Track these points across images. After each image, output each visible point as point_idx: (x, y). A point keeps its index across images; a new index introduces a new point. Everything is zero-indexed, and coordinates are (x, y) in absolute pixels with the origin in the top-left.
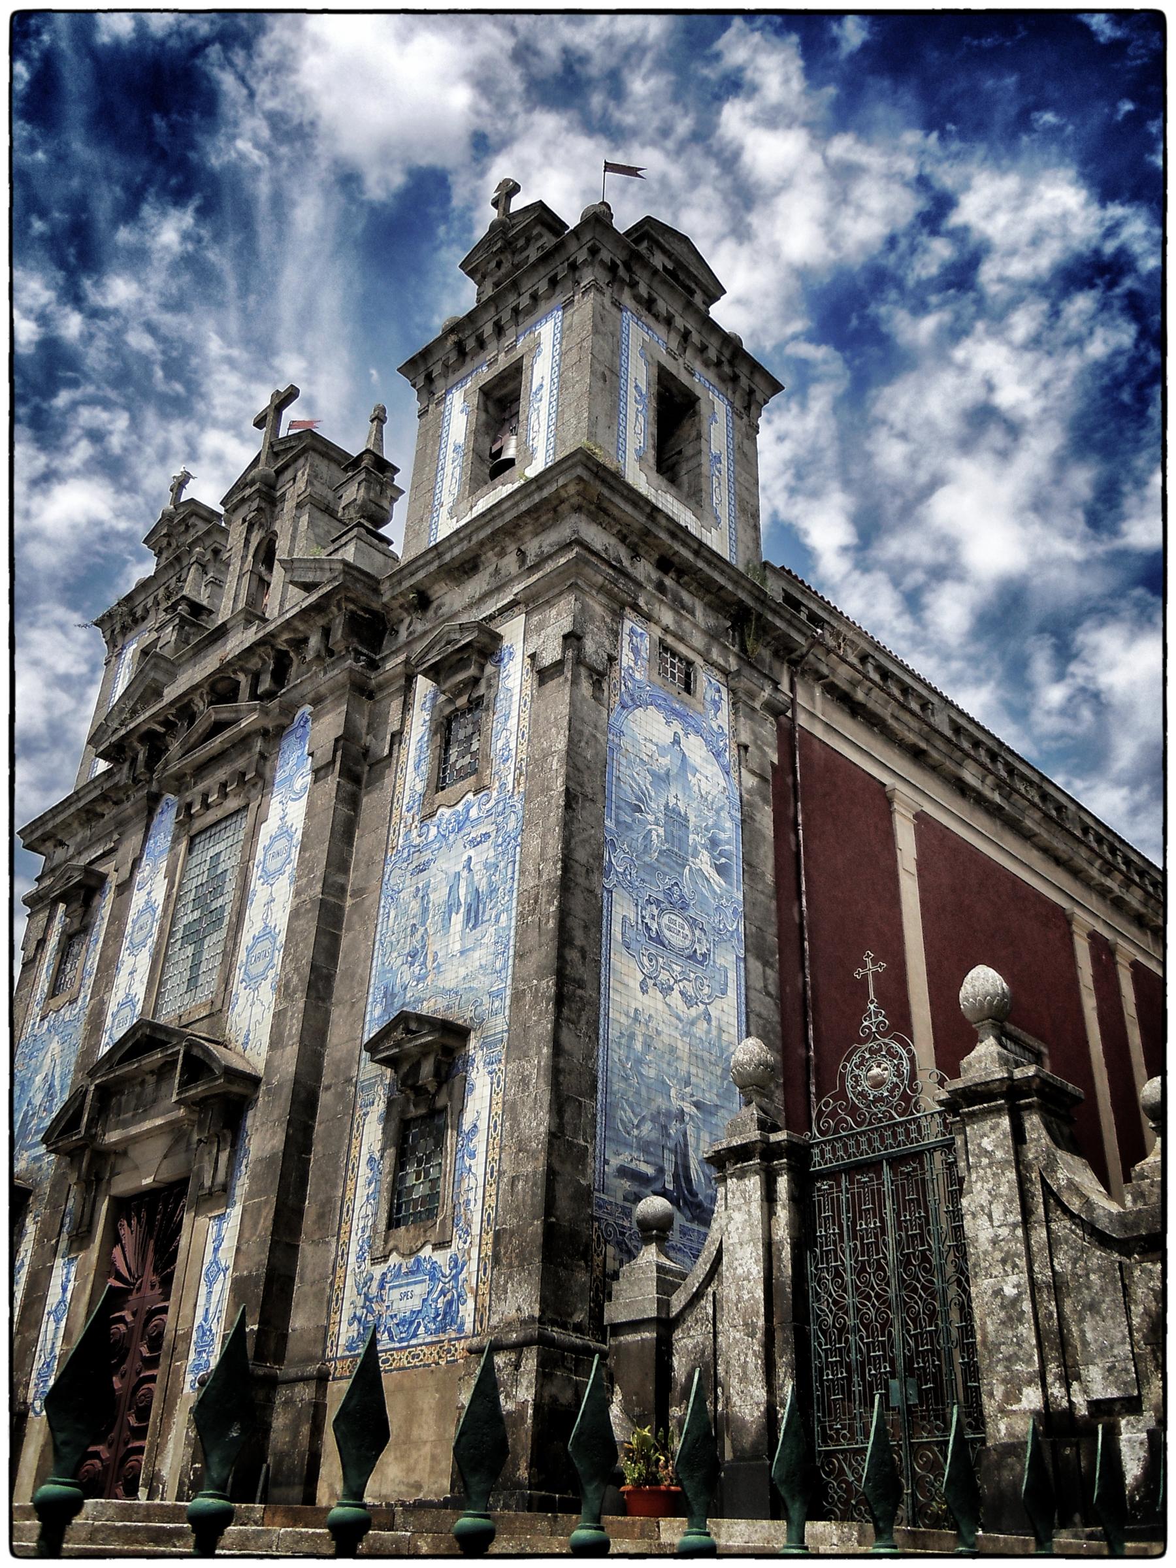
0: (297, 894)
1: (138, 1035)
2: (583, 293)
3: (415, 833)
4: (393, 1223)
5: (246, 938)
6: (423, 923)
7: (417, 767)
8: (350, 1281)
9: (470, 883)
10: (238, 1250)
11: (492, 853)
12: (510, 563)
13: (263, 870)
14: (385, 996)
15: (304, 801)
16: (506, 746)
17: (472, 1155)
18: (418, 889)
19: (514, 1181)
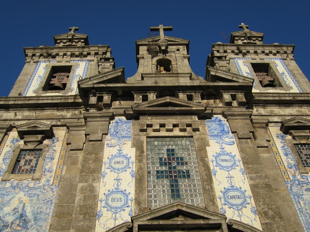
0: (251, 179)
1: (175, 209)
2: (291, 60)
7: (286, 155)
13: (217, 163)
15: (235, 147)
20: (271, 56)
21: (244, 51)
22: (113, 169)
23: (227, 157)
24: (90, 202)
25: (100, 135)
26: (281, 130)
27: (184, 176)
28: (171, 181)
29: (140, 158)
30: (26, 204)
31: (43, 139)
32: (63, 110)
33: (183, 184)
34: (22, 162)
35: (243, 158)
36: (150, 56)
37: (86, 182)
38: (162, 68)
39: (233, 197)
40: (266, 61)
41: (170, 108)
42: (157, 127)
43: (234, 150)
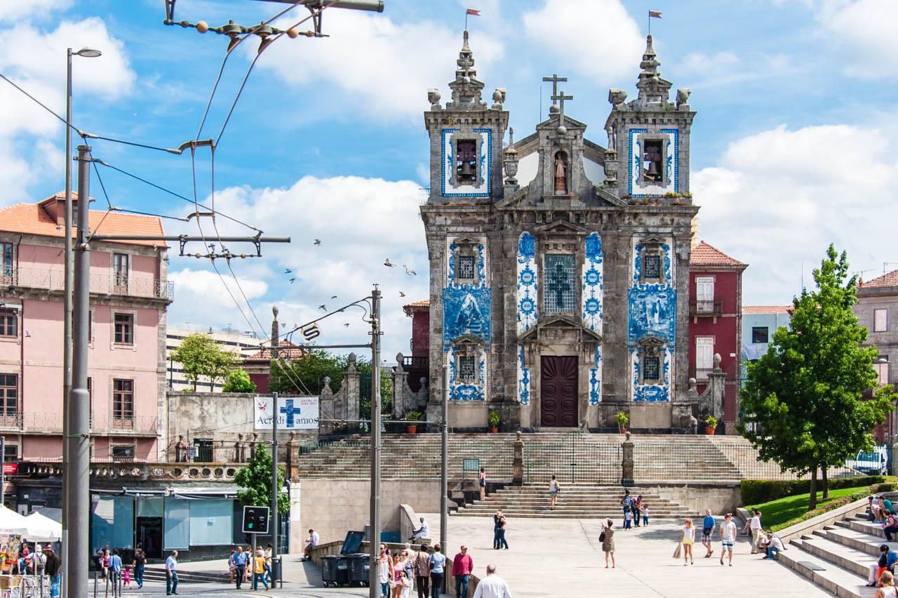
0: (605, 293)
3: (638, 286)
4: (644, 378)
5: (584, 299)
6: (645, 312)
7: (636, 266)
8: (633, 388)
9: (660, 307)
10: (603, 378)
11: (666, 302)
12: (668, 219)
14: (634, 325)
16: (669, 274)
17: (667, 369)
18: (641, 303)
19: (680, 376)
20: (669, 127)
21: (642, 120)
22: (524, 283)
23: (594, 275)
24: (512, 307)
25: (514, 252)
26: (641, 241)
27: (566, 289)
28: (558, 293)
29: (540, 273)
30: (475, 303)
31: (473, 246)
32: (481, 215)
33: (565, 295)
34: (463, 267)
35: (604, 276)
36: (549, 148)
37: (509, 292)
38: (559, 157)
39: (591, 306)
40: (661, 136)
41: (561, 233)
42: (551, 247)
43: (599, 268)
